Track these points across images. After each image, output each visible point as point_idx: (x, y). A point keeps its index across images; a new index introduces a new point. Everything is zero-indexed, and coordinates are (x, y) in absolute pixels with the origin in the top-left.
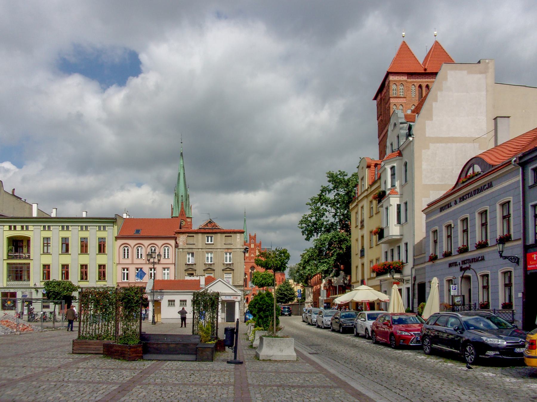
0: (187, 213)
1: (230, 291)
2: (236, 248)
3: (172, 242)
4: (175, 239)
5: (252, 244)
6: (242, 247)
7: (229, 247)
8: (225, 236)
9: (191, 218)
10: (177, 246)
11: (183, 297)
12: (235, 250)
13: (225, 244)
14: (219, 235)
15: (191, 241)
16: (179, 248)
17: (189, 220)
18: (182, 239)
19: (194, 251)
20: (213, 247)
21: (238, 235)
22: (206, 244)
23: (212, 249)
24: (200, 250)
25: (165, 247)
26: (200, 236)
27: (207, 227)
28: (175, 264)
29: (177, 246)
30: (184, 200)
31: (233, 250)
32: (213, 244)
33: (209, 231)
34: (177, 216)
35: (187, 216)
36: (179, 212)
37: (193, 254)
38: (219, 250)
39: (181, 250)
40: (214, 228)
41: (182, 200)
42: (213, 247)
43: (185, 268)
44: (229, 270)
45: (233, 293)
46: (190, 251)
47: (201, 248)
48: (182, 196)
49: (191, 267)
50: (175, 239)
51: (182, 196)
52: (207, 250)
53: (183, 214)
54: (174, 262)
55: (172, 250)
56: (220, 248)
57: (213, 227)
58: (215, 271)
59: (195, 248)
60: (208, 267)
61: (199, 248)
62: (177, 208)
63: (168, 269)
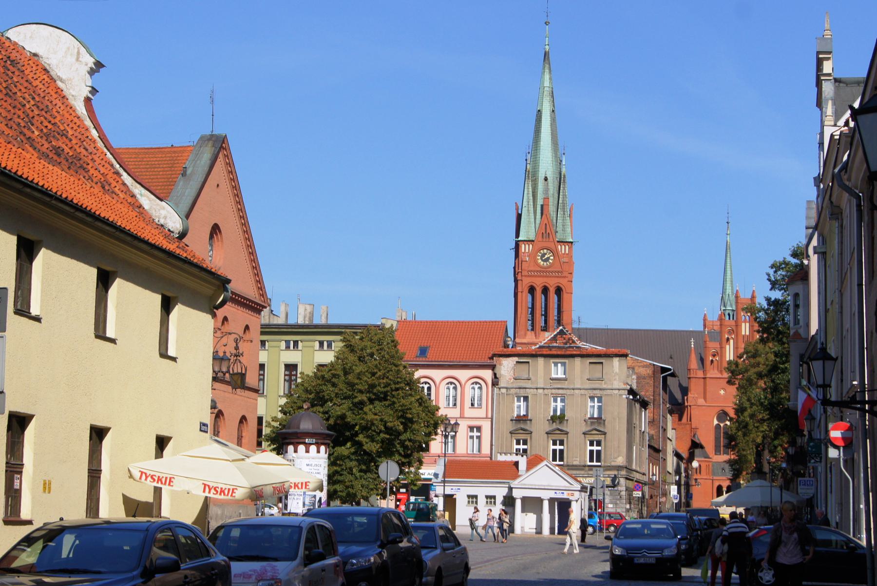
0: (559, 228)
1: (562, 484)
2: (610, 387)
3: (487, 374)
4: (493, 367)
5: (745, 322)
6: (623, 386)
7: (596, 385)
8: (590, 363)
9: (572, 243)
10: (495, 382)
11: (491, 491)
12: (609, 392)
13: (589, 380)
14: (578, 361)
15: (523, 371)
16: (499, 386)
17: (563, 249)
18: (507, 366)
19: (530, 393)
20: (565, 385)
21: (616, 360)
22: (552, 379)
23: (563, 389)
24: (540, 391)
25: (473, 384)
26: (541, 360)
27: (555, 344)
28: (492, 419)
29: (495, 382)
30: (551, 192)
31: (605, 392)
32: (565, 379)
33: (559, 353)
34: (532, 237)
35: (559, 237)
36: (537, 226)
37: (526, 399)
38: (577, 391)
39: (504, 391)
40: (568, 345)
41: (546, 190)
42: (565, 385)
43: (511, 427)
44: (597, 433)
45: (568, 487)
46: (522, 392)
47: (542, 386)
48: (546, 179)
49: (523, 426)
50: (493, 367)
51: (546, 179)
52: (554, 391)
53: (548, 231)
54: (490, 416)
55: (487, 390)
56: (579, 387)
57: (566, 343)
58: (569, 434)
59: (530, 386)
60: (555, 426)
61: (538, 386)
62: (532, 215)
63: (479, 429)
